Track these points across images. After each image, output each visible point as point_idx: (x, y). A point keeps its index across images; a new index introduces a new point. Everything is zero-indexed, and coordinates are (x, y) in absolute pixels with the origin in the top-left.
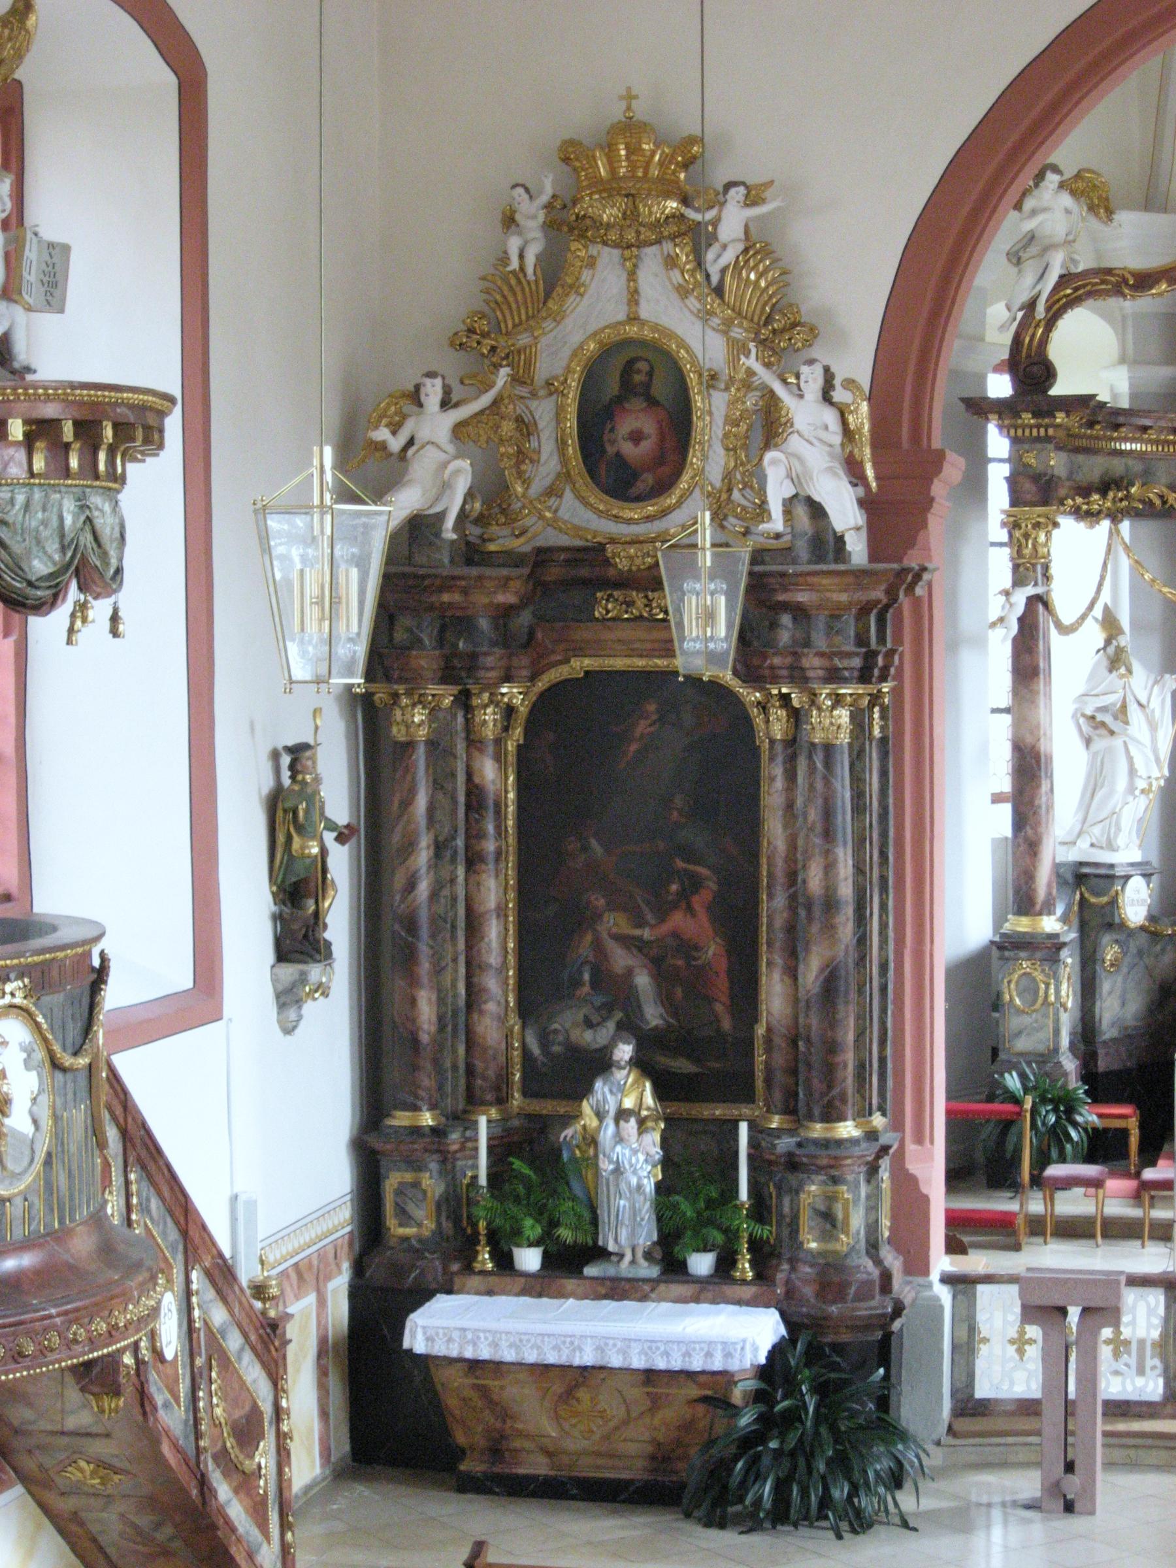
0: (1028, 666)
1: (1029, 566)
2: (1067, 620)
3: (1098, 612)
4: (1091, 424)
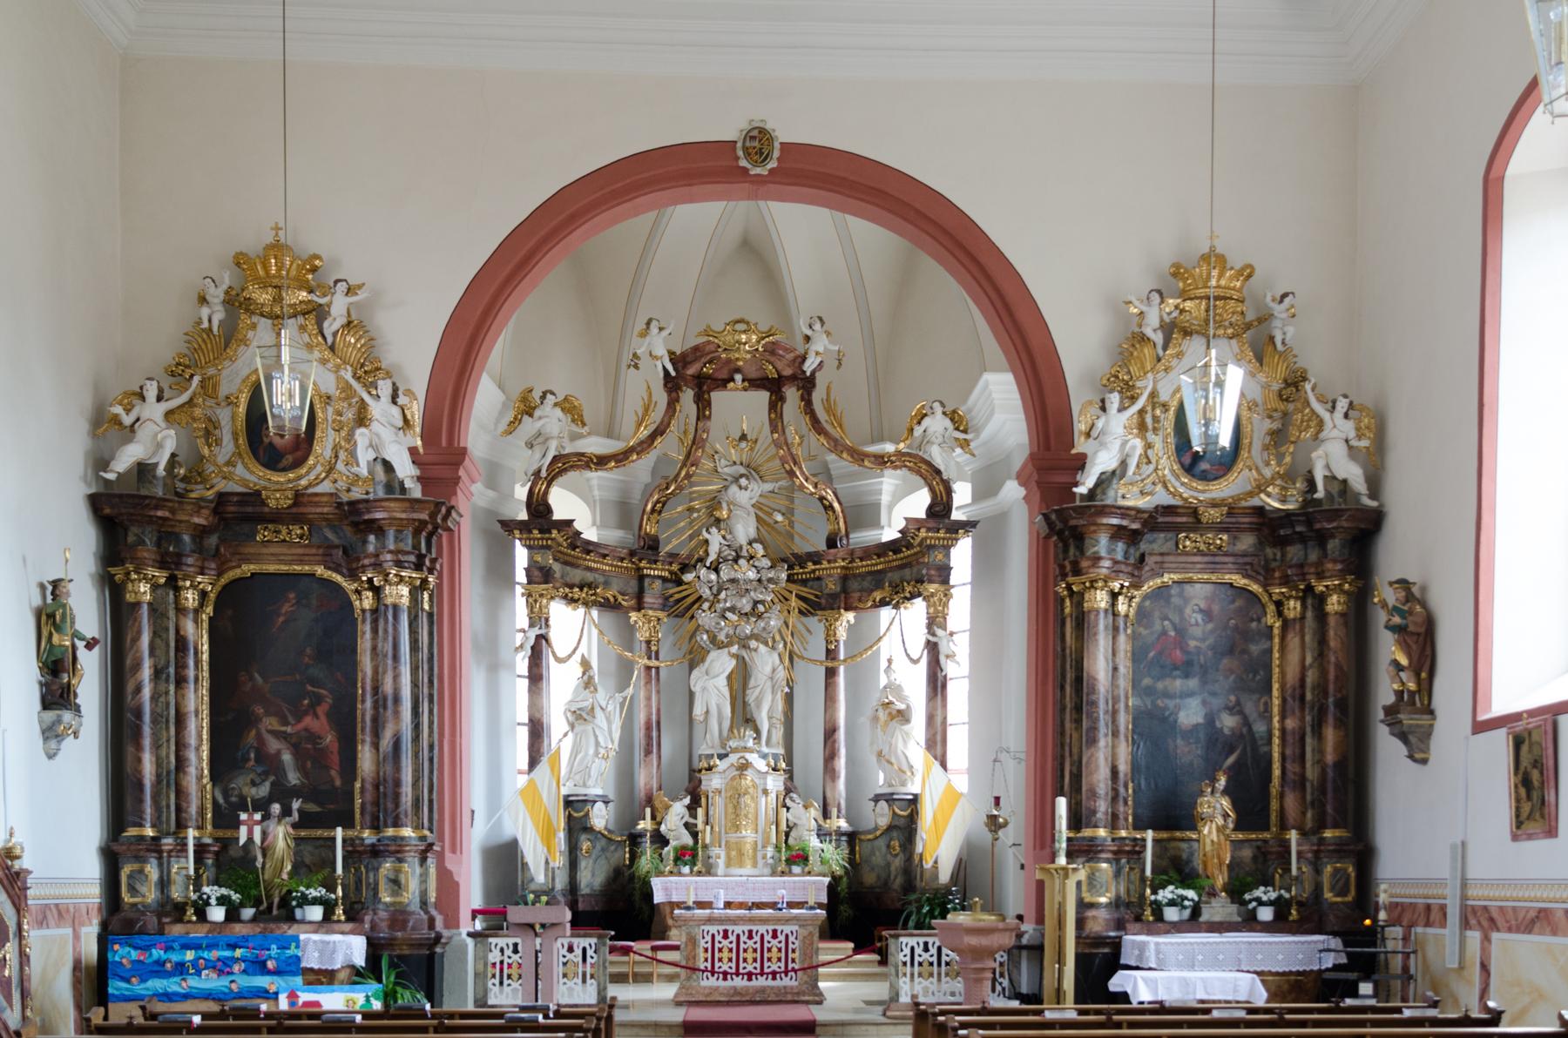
0: (536, 676)
1: (538, 618)
2: (561, 654)
3: (577, 657)
4: (574, 547)
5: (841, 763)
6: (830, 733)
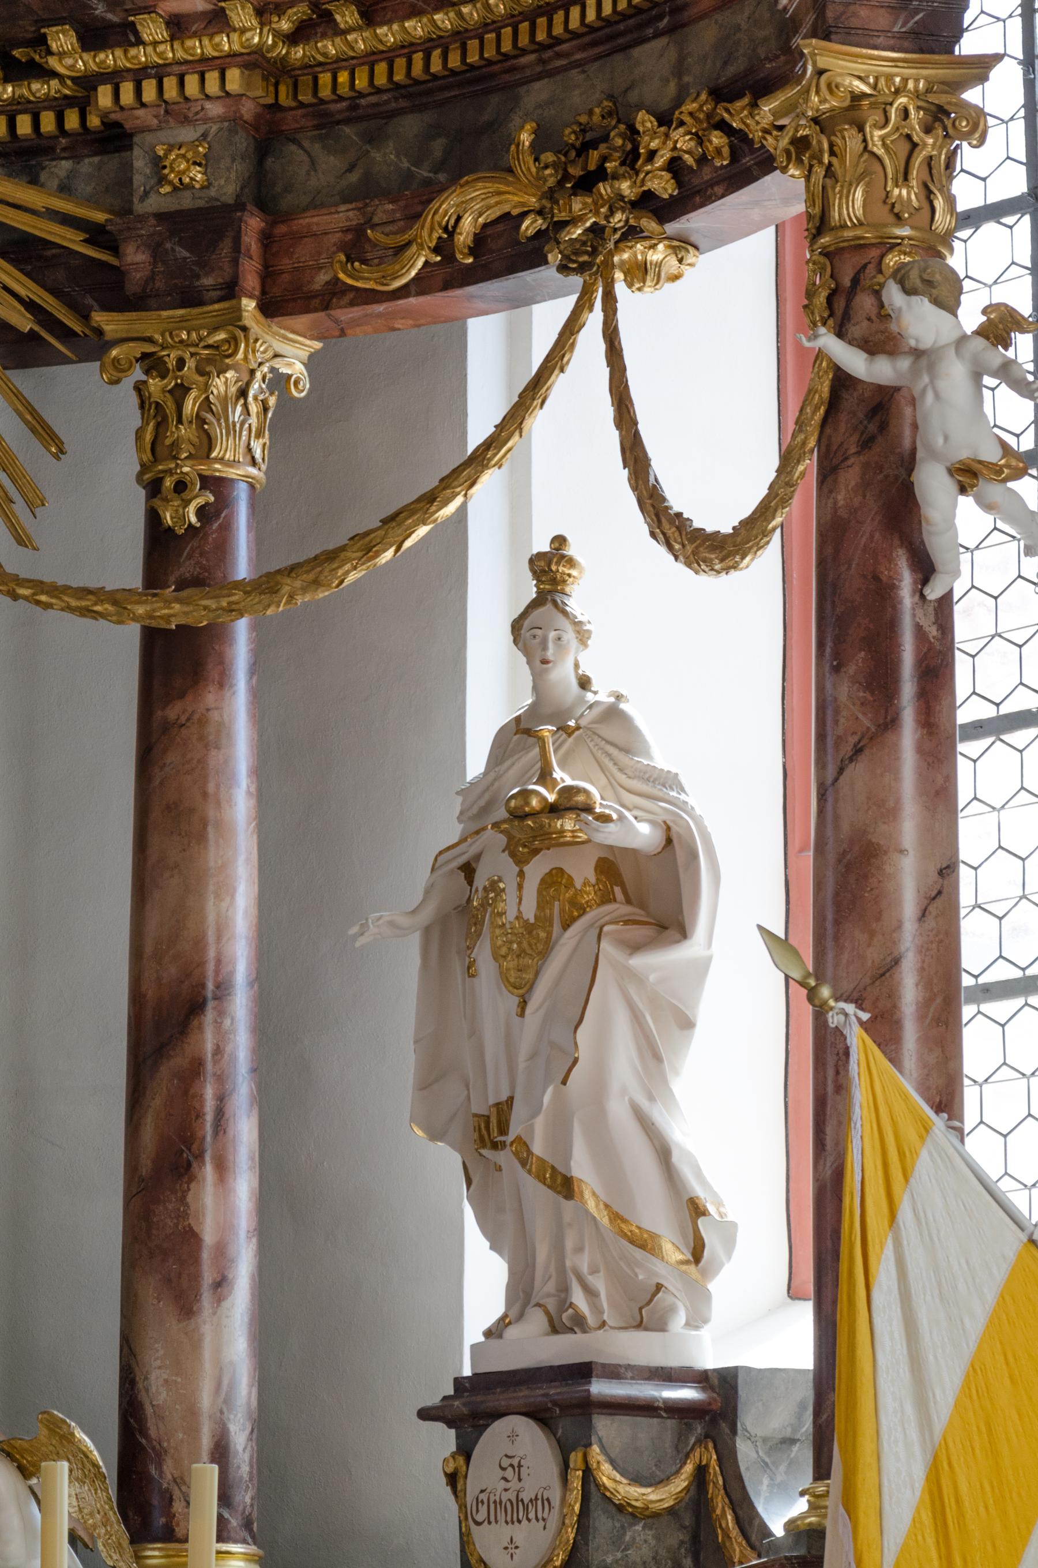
5: (231, 1204)
6: (166, 1017)
